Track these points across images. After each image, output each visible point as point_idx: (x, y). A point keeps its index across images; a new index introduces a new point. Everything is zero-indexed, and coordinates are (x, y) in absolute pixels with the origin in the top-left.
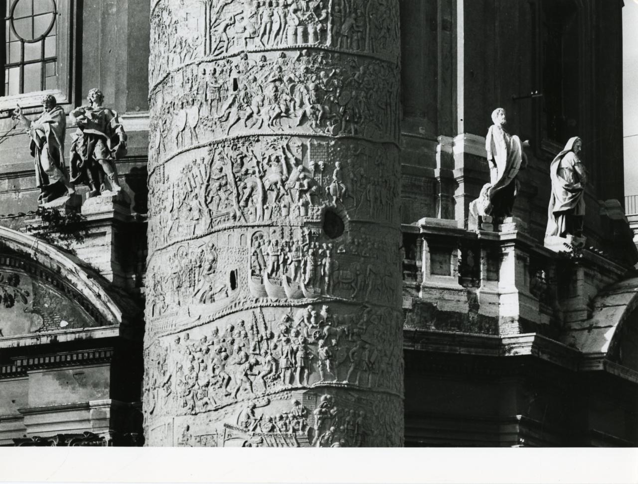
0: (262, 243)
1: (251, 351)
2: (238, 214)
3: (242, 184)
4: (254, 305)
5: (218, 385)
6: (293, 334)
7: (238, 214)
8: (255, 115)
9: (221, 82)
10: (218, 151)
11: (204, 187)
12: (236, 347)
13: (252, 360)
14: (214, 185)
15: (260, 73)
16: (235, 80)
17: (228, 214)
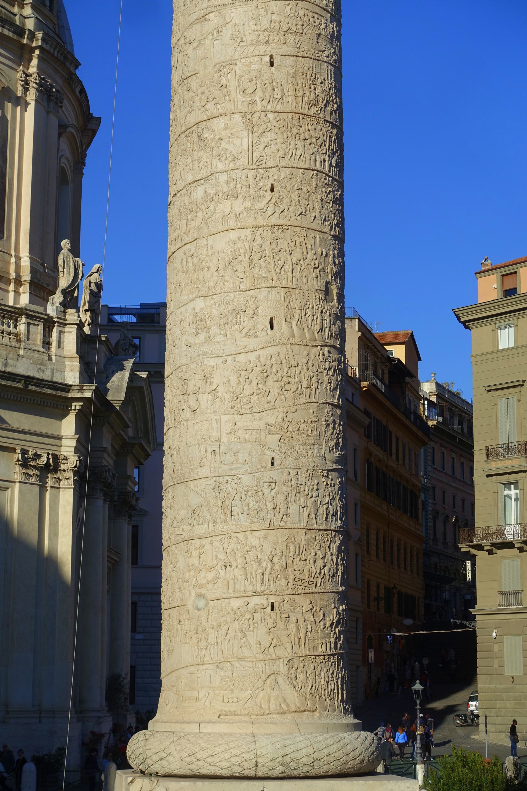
0: (291, 300)
1: (285, 374)
2: (275, 278)
3: (278, 258)
4: (286, 342)
5: (261, 395)
6: (310, 363)
7: (275, 278)
8: (286, 211)
9: (261, 184)
10: (258, 233)
11: (247, 257)
12: (274, 370)
13: (285, 380)
14: (256, 257)
15: (289, 183)
16: (272, 185)
17: (267, 277)
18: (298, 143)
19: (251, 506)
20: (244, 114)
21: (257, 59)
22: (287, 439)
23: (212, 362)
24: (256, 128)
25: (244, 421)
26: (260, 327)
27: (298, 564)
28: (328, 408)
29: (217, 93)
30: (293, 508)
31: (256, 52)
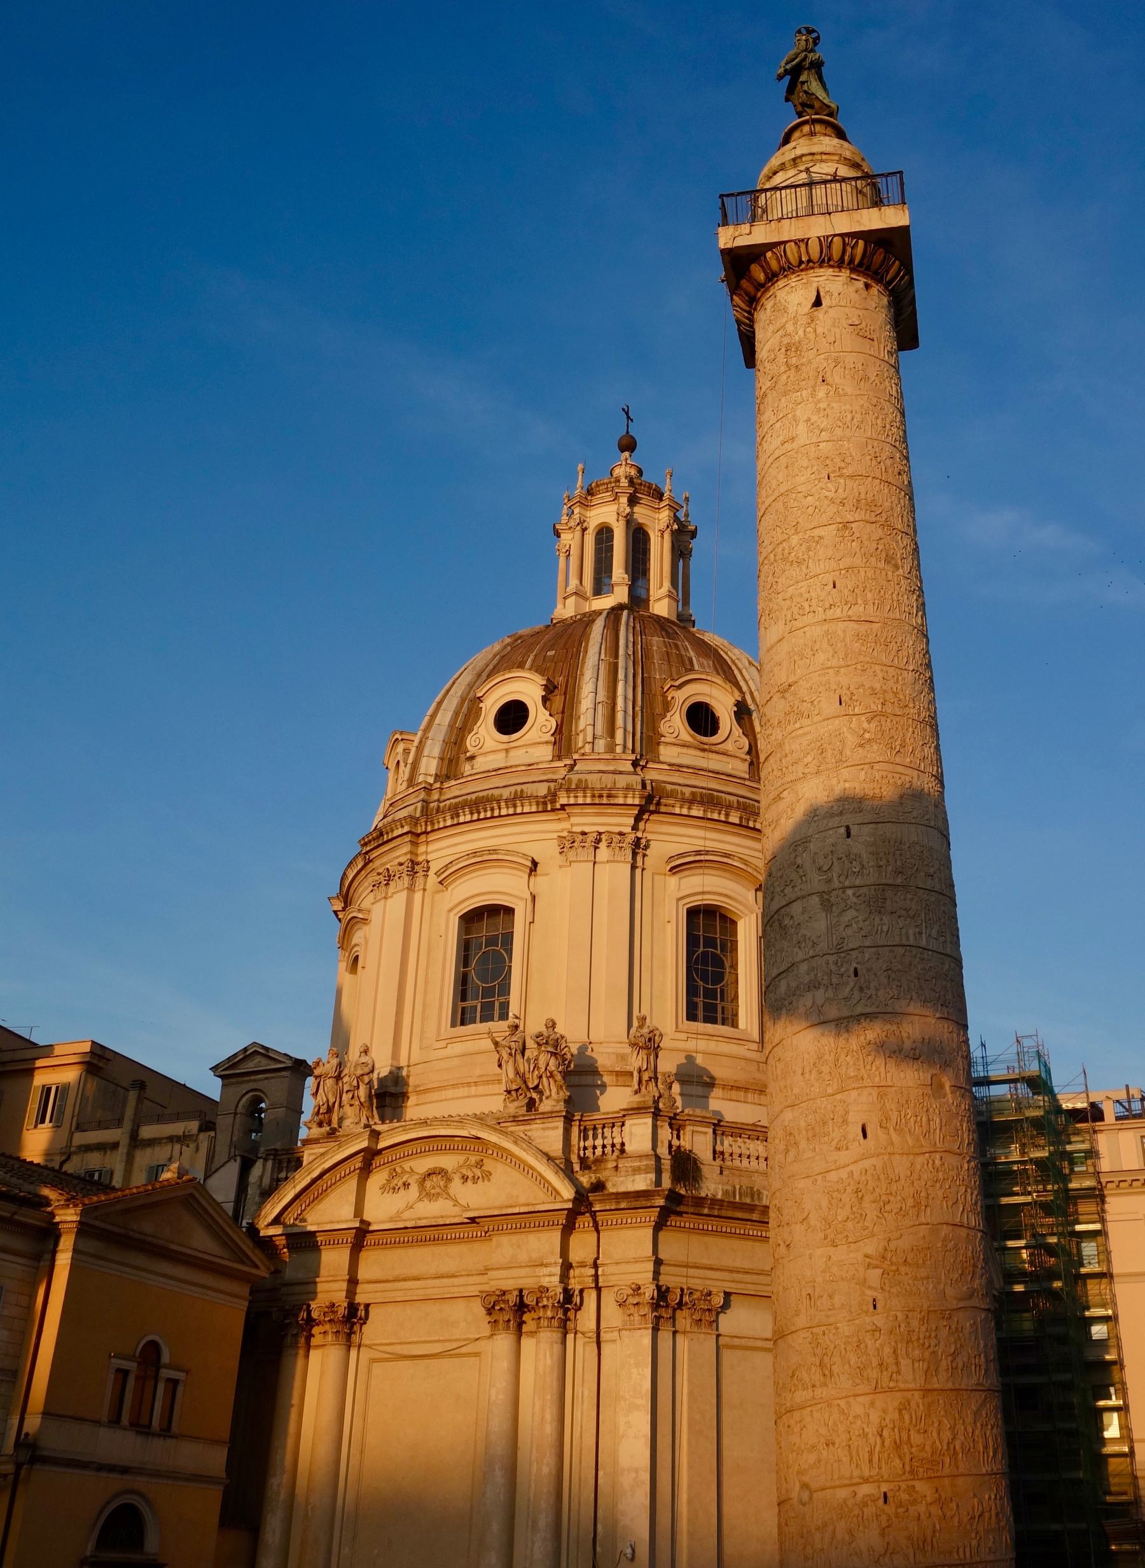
2: (866, 1076)
4: (883, 1151)
5: (856, 1220)
6: (915, 1176)
7: (866, 1076)
12: (870, 1187)
18: (884, 917)
19: (852, 1363)
20: (820, 894)
21: (831, 832)
22: (891, 1274)
23: (801, 1184)
24: (834, 908)
25: (841, 1254)
26: (851, 1137)
27: (916, 1438)
28: (945, 1229)
29: (794, 876)
30: (904, 1362)
31: (831, 825)
